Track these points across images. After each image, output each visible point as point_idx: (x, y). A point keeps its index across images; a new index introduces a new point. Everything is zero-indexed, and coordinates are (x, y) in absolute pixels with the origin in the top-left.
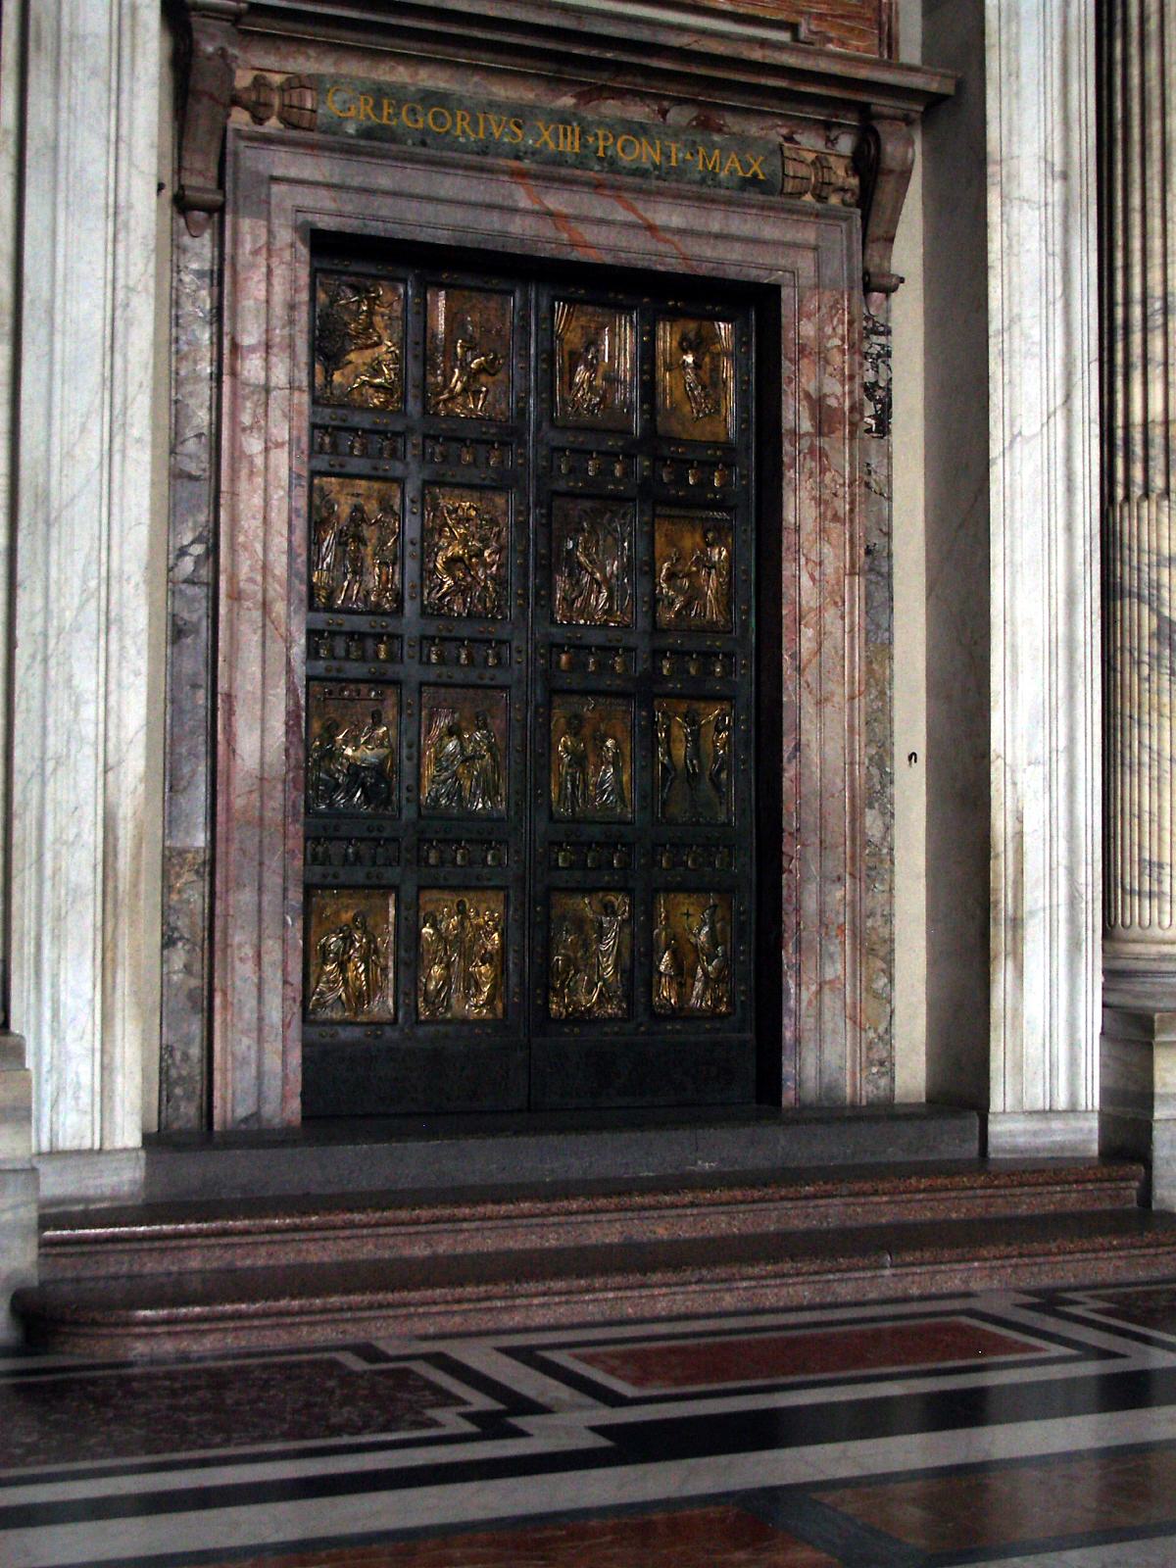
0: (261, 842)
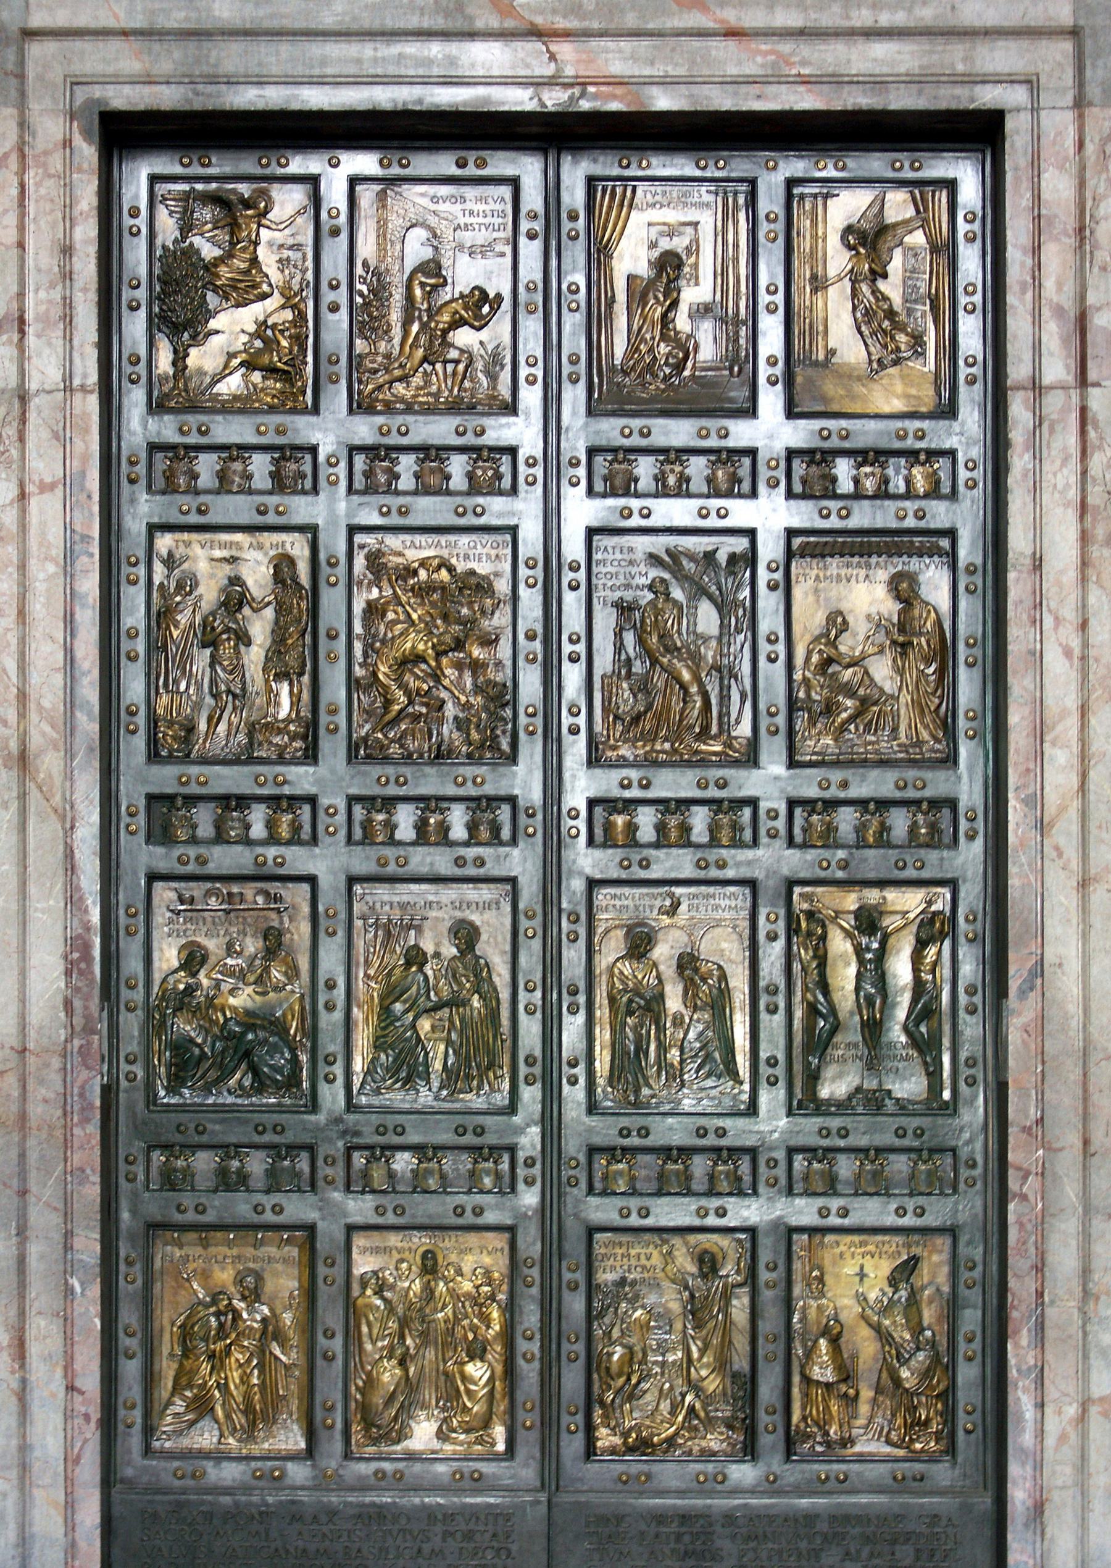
0: (22, 1155)
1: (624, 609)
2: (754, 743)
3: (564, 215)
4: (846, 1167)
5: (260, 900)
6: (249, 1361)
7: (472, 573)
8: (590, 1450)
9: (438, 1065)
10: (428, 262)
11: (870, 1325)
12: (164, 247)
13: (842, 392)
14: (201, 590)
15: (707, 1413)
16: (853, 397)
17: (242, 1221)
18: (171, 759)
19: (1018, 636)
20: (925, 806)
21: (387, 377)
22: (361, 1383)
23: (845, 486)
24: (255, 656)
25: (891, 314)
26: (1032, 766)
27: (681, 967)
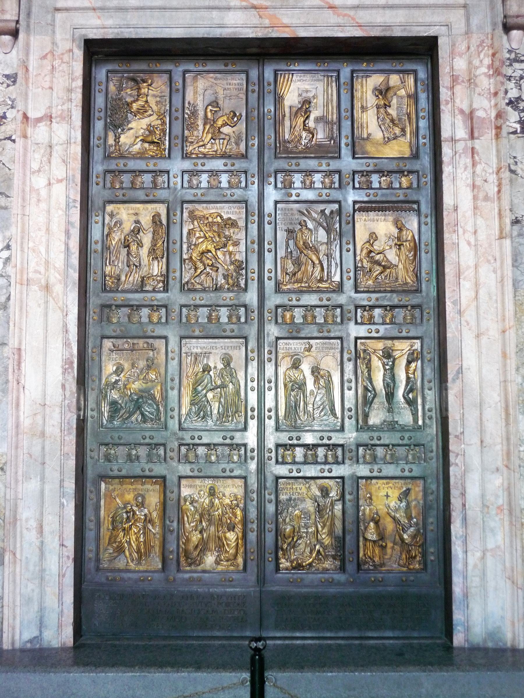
0: (43, 448)
1: (290, 232)
2: (341, 284)
3: (266, 84)
5: (145, 345)
6: (139, 531)
7: (230, 219)
8: (277, 569)
9: (215, 412)
10: (213, 102)
12: (112, 97)
13: (374, 149)
14: (124, 226)
15: (325, 553)
16: (378, 151)
17: (136, 474)
18: (111, 291)
19: (448, 237)
20: (409, 308)
21: (197, 145)
23: (376, 185)
25: (392, 121)
26: (455, 289)
27: (313, 372)
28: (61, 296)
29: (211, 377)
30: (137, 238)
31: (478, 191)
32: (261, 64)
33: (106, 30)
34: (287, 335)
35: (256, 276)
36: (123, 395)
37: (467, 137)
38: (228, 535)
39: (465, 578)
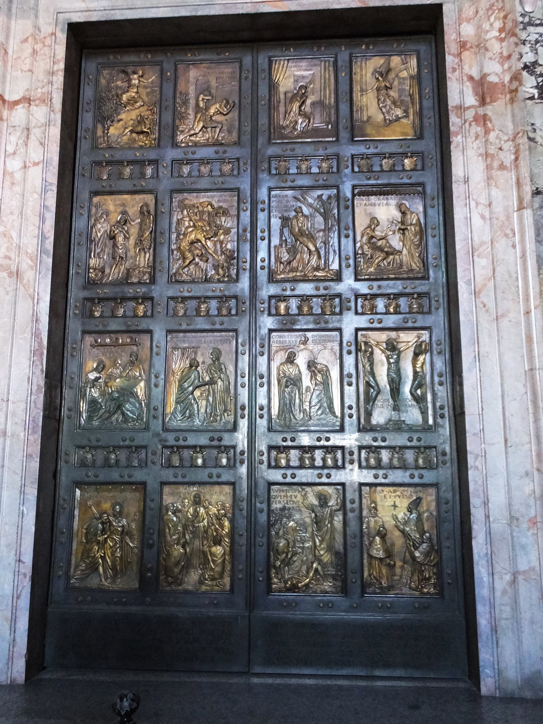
4: (385, 455)
5: (128, 340)
7: (221, 207)
8: (269, 590)
9: (203, 410)
11: (399, 530)
14: (111, 217)
17: (115, 481)
22: (165, 556)
24: (132, 241)
28: (32, 283)
29: (198, 371)
30: (124, 229)
31: (492, 160)
32: (255, 53)
33: (91, 13)
34: (280, 327)
35: (248, 265)
36: (103, 394)
37: (477, 104)
38: (214, 549)
39: (492, 606)
